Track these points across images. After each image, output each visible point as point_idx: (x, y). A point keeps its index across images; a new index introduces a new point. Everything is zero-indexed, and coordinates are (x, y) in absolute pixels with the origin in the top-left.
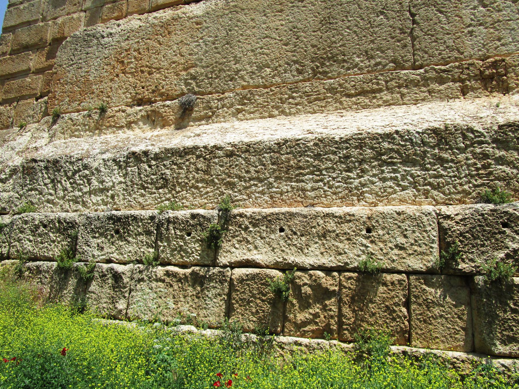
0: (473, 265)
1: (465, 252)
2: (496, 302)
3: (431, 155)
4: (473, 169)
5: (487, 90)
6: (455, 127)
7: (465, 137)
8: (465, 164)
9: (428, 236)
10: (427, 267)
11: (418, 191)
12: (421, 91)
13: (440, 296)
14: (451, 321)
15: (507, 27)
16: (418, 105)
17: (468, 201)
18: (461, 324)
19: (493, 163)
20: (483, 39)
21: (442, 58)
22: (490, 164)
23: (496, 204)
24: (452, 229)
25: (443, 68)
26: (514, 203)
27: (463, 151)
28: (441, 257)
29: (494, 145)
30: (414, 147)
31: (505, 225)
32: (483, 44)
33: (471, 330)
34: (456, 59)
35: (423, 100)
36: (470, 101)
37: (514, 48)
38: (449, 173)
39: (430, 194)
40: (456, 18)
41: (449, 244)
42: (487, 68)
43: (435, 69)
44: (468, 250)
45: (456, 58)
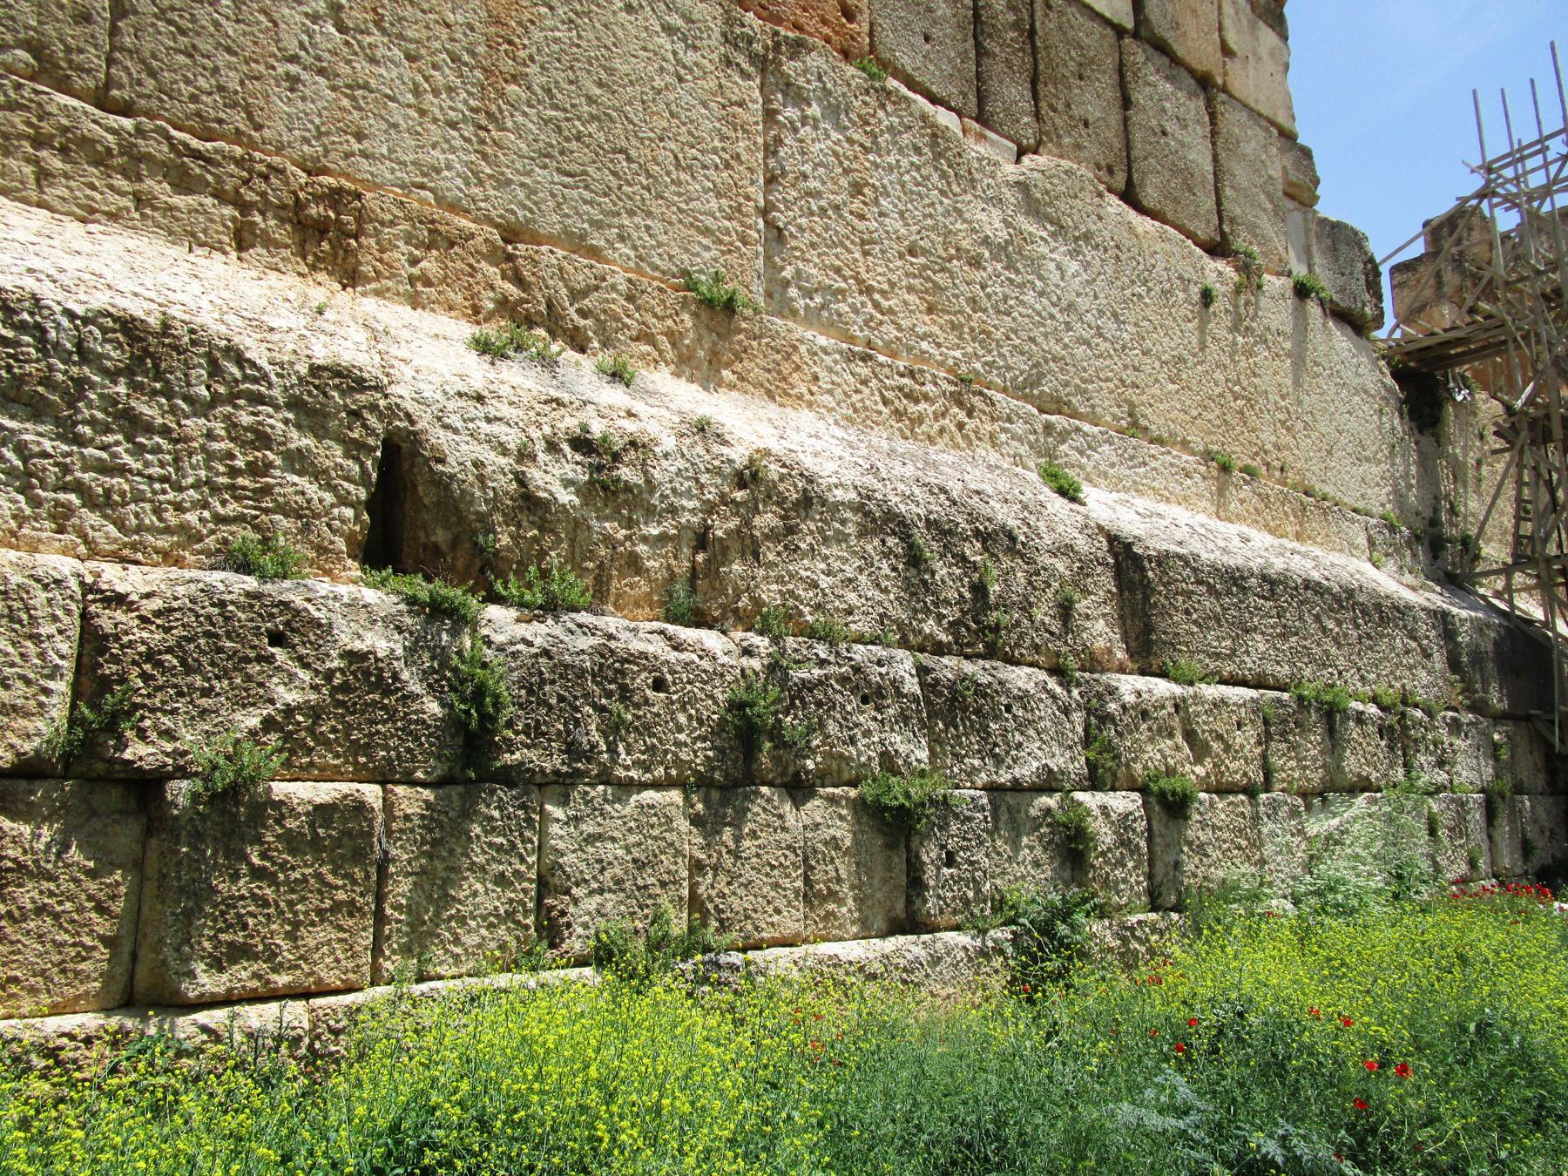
0: (169, 747)
1: (153, 710)
2: (215, 854)
3: (101, 396)
4: (222, 469)
5: (304, 259)
6: (192, 331)
7: (215, 370)
8: (203, 449)
9: (42, 655)
10: (18, 755)
11: (36, 502)
12: (111, 187)
13: (48, 846)
14: (73, 921)
15: (383, 112)
16: (92, 227)
17: (190, 558)
18: (103, 926)
19: (278, 462)
20: (320, 115)
21: (198, 114)
22: (269, 465)
23: (263, 578)
24: (125, 639)
25: (195, 143)
27: (202, 408)
28: (72, 722)
29: (291, 416)
30: (46, 355)
31: (277, 639)
32: (317, 128)
33: (129, 947)
34: (238, 137)
35: (113, 217)
36: (255, 274)
37: (389, 176)
38: (147, 464)
39: (76, 520)
40: (262, 18)
41: (105, 684)
42: (318, 198)
43: (169, 138)
44: (163, 702)
45: (238, 131)
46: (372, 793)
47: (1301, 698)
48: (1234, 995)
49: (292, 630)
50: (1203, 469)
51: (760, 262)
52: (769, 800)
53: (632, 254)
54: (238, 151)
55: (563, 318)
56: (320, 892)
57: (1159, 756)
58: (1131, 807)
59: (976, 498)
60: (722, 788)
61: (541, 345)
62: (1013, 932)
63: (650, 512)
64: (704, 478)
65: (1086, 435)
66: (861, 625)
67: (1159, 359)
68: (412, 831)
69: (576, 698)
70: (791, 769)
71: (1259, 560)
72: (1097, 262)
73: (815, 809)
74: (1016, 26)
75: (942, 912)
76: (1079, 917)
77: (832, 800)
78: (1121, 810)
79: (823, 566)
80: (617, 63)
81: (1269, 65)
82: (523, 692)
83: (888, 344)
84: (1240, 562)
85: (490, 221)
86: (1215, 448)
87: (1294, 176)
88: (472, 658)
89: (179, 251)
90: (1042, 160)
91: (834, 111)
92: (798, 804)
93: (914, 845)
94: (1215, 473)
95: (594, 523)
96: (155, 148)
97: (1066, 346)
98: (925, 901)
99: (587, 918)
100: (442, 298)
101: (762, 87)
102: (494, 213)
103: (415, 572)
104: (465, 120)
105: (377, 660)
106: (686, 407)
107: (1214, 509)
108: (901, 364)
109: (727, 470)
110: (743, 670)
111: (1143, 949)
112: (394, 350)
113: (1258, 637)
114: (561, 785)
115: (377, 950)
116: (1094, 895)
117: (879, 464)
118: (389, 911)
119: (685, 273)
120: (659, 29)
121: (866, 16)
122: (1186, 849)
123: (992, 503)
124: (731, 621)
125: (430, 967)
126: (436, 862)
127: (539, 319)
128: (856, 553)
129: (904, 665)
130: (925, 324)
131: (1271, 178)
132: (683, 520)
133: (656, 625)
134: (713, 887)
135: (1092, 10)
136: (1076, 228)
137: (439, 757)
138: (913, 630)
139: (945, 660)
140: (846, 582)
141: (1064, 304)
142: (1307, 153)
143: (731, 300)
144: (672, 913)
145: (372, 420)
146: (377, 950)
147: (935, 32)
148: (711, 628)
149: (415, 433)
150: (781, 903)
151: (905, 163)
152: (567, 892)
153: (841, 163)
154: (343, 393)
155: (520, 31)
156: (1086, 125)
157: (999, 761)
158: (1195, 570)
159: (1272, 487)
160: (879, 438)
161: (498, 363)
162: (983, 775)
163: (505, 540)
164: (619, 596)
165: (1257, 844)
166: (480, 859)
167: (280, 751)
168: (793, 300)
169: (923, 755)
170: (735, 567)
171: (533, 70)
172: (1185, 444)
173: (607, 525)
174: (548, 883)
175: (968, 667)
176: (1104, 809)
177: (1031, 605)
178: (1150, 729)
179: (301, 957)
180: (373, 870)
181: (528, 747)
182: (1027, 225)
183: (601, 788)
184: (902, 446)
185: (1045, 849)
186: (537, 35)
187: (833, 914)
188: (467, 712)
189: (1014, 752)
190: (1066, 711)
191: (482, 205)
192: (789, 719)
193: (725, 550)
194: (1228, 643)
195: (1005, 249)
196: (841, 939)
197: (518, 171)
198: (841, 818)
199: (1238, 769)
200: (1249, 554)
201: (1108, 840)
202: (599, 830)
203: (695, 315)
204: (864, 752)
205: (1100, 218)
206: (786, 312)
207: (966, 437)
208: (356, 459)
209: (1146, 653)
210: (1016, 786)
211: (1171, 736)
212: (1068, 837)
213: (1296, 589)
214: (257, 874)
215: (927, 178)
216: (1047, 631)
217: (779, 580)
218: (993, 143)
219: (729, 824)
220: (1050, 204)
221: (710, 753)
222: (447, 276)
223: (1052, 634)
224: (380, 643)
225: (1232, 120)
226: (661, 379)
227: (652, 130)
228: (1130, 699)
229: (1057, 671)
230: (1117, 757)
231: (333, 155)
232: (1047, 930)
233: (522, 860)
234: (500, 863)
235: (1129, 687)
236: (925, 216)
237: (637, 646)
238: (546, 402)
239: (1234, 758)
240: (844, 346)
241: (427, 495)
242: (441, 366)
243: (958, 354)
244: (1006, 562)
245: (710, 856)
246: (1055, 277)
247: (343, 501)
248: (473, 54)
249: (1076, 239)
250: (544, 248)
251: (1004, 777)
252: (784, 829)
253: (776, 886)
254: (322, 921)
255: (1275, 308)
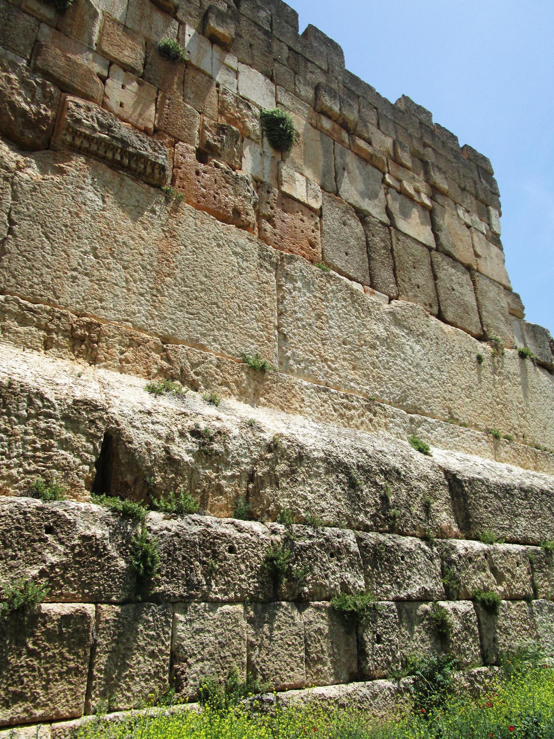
2: (10, 643)
5: (74, 352)
6: (22, 386)
7: (31, 403)
8: (22, 439)
15: (112, 290)
19: (56, 444)
20: (85, 292)
21: (32, 293)
22: (52, 446)
25: (30, 305)
26: (66, 501)
27: (23, 420)
29: (63, 423)
31: (49, 530)
32: (83, 297)
36: (51, 360)
37: (113, 317)
40: (63, 253)
42: (81, 327)
43: (19, 303)
46: (90, 608)
47: (547, 550)
48: (531, 712)
49: (57, 525)
50: (486, 437)
51: (276, 350)
52: (286, 609)
53: (219, 347)
54: (48, 308)
55: (188, 376)
56: (61, 662)
57: (479, 581)
58: (468, 609)
59: (380, 454)
60: (263, 603)
61: (177, 388)
62: (413, 679)
63: (227, 465)
64: (252, 448)
65: (429, 423)
66: (328, 517)
67: (460, 387)
68: (109, 628)
69: (191, 557)
70: (297, 592)
71: (518, 481)
72: (428, 345)
73: (309, 613)
74: (385, 248)
75: (376, 667)
76: (447, 670)
77: (318, 608)
78: (463, 610)
79: (309, 489)
80: (213, 268)
81: (496, 261)
82: (166, 554)
83: (335, 384)
84: (509, 482)
85: (156, 334)
86: (491, 427)
87: (513, 306)
88: (142, 538)
89: (19, 351)
90: (400, 302)
91: (308, 284)
92: (301, 611)
93: (360, 632)
94: (492, 439)
95: (201, 470)
96: (14, 308)
97: (417, 383)
98: (367, 663)
99: (195, 675)
100: (134, 368)
101: (276, 276)
102: (158, 331)
103: (116, 496)
104: (147, 292)
105: (97, 540)
106: (244, 415)
107: (493, 456)
108: (342, 393)
109: (263, 443)
110: (272, 541)
111: (482, 687)
112: (112, 392)
113: (522, 519)
114: (182, 603)
115: (88, 695)
116: (454, 657)
117: (334, 439)
118: (95, 673)
119: (243, 355)
120: (231, 253)
121: (320, 246)
122: (498, 631)
123: (388, 456)
124: (266, 517)
125: (115, 704)
126: (120, 645)
127: (177, 377)
128: (324, 482)
129: (350, 537)
130: (352, 374)
131: (502, 307)
132: (243, 468)
133: (230, 520)
134: (259, 657)
135: (417, 240)
136: (418, 331)
137: (123, 589)
138: (354, 520)
139: (370, 534)
140: (320, 496)
141: (415, 364)
142: (517, 296)
143: (264, 366)
144: (238, 672)
145: (100, 424)
146: (88, 695)
147: (350, 251)
148: (256, 520)
149: (119, 430)
150: (294, 665)
151: (339, 305)
152: (185, 661)
153: (311, 306)
154: (88, 412)
155: (172, 256)
156: (418, 287)
157: (400, 585)
158: (487, 486)
159: (520, 446)
160: (333, 427)
161: (158, 397)
162: (392, 593)
163: (159, 479)
164: (212, 506)
165: (534, 627)
166: (142, 643)
167: (46, 587)
168: (291, 365)
169: (362, 583)
170: (267, 490)
171: (177, 271)
172: (476, 426)
173: (207, 471)
174: (177, 656)
175: (382, 538)
176: (454, 610)
177: (410, 505)
178: (474, 567)
179: (49, 700)
180: (88, 650)
181: (167, 583)
182: (396, 330)
183: (203, 604)
184: (344, 431)
185: (427, 633)
186: (179, 257)
187: (319, 671)
188: (138, 566)
189: (407, 581)
190: (431, 559)
191: (153, 328)
192: (295, 566)
193: (262, 482)
194: (507, 522)
195: (386, 340)
196: (325, 685)
197: (169, 313)
198: (323, 618)
199: (521, 587)
200: (513, 478)
201: (458, 627)
202: (202, 626)
203: (247, 373)
204: (333, 582)
205: (428, 326)
206: (289, 371)
207: (374, 426)
208: (92, 443)
209: (468, 529)
210: (409, 599)
211: (484, 570)
212: (438, 626)
213: (537, 494)
214: (31, 653)
215: (349, 311)
216: (419, 518)
217: (289, 496)
218: (378, 296)
219: (267, 622)
220: (405, 321)
221: (257, 585)
222: (136, 359)
223: (421, 520)
224: (98, 531)
225: (482, 283)
226: (232, 402)
227: (228, 294)
228: (462, 552)
229: (425, 538)
230: (459, 582)
231: (89, 308)
232: (431, 677)
233: (163, 644)
234: (152, 645)
235: (461, 546)
236: (349, 327)
237: (221, 530)
238: (179, 414)
239: (517, 582)
240: (315, 385)
241: (123, 458)
242: (132, 399)
243: (368, 388)
244: (397, 485)
245: (257, 640)
246: (410, 352)
247: (85, 462)
248: (152, 266)
249: (418, 335)
250: (180, 346)
251: (403, 595)
252: (294, 624)
253: (291, 655)
254: (61, 679)
255: (511, 363)
